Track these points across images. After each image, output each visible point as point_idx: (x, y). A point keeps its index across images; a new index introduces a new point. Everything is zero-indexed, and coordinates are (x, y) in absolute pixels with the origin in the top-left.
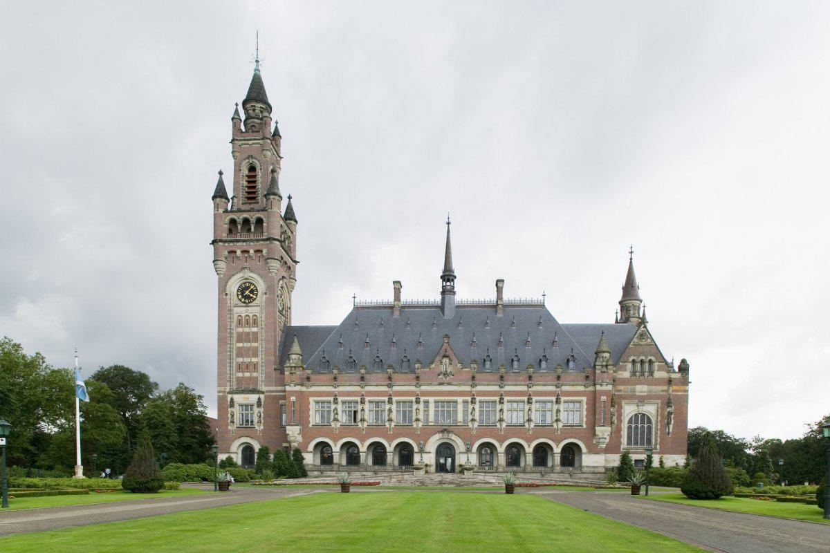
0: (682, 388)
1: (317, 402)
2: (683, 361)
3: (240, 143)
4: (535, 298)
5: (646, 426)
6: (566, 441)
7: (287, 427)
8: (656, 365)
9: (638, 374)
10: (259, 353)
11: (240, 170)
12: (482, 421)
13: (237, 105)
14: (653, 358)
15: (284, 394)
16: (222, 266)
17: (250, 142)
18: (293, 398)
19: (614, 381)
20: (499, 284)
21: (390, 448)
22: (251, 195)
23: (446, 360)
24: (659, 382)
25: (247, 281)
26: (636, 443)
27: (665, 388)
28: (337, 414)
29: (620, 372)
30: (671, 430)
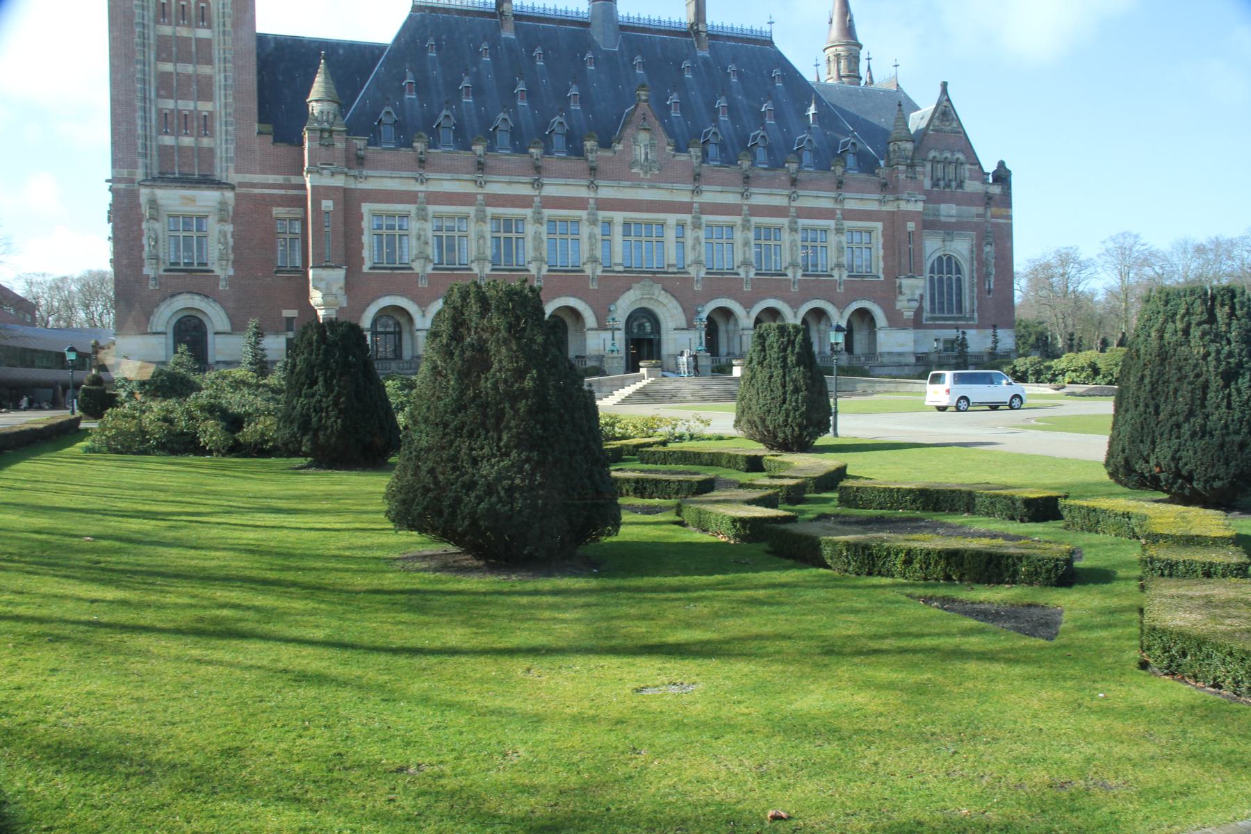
0: (1003, 211)
1: (378, 215)
2: (1001, 164)
4: (756, 27)
5: (954, 277)
9: (942, 183)
10: (219, 93)
14: (961, 157)
23: (643, 137)
24: (970, 199)
26: (942, 310)
27: (981, 210)
28: (426, 243)
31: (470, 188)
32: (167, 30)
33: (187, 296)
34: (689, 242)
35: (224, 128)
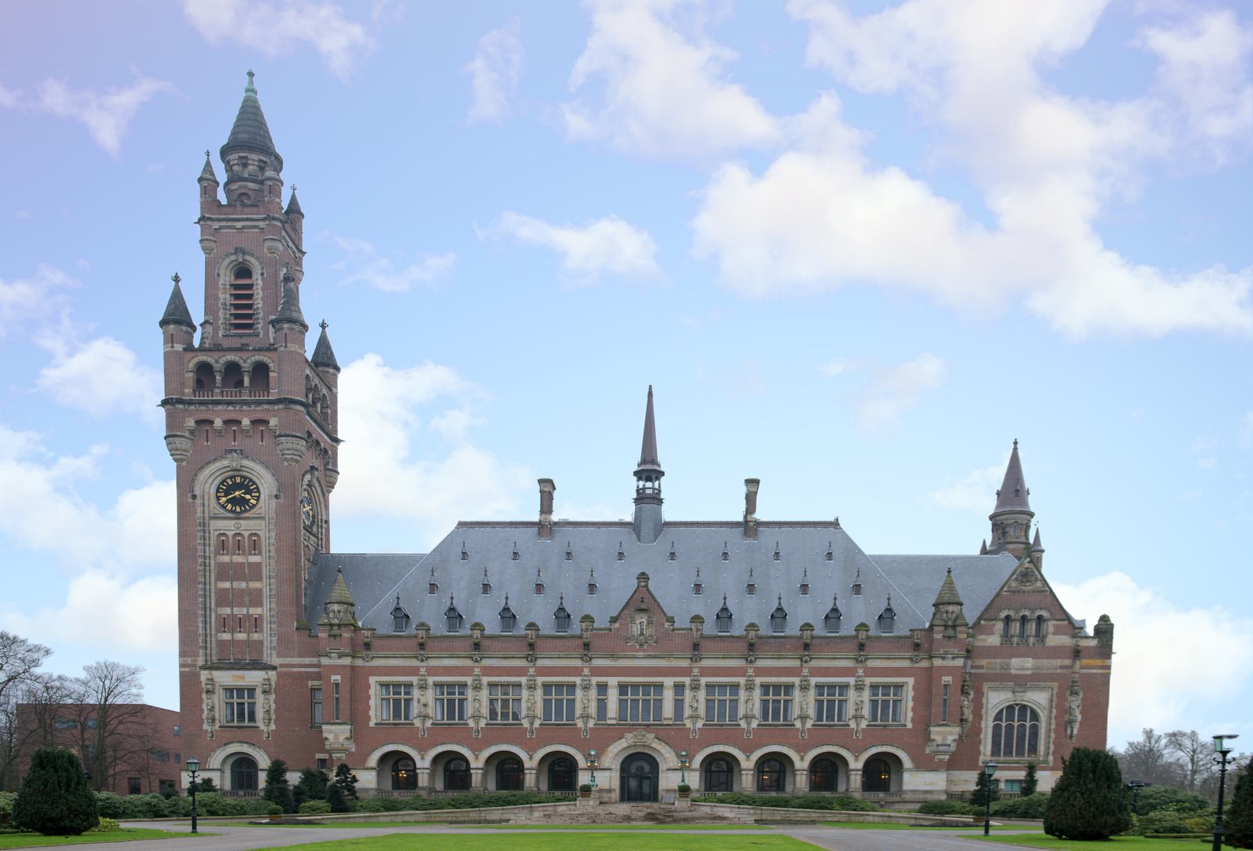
1: (385, 686)
3: (216, 225)
10: (266, 601)
11: (218, 275)
16: (184, 447)
17: (239, 225)
22: (243, 317)
25: (236, 473)
32: (226, 559)
35: (269, 625)
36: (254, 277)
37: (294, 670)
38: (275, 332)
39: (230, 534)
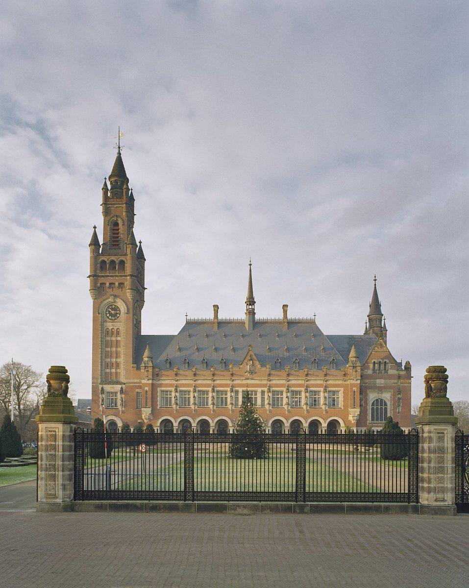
0: (407, 381)
2: (408, 363)
5: (383, 407)
6: (331, 419)
7: (143, 409)
8: (389, 366)
10: (122, 356)
12: (274, 405)
13: (105, 179)
14: (387, 361)
15: (141, 384)
18: (147, 388)
19: (361, 377)
20: (285, 307)
21: (212, 424)
24: (391, 377)
26: (377, 420)
27: (396, 381)
28: (177, 399)
29: (366, 370)
30: (400, 411)
31: (192, 382)
33: (111, 416)
34: (266, 397)
36: (120, 226)
37: (131, 385)
38: (126, 248)
39: (110, 328)
